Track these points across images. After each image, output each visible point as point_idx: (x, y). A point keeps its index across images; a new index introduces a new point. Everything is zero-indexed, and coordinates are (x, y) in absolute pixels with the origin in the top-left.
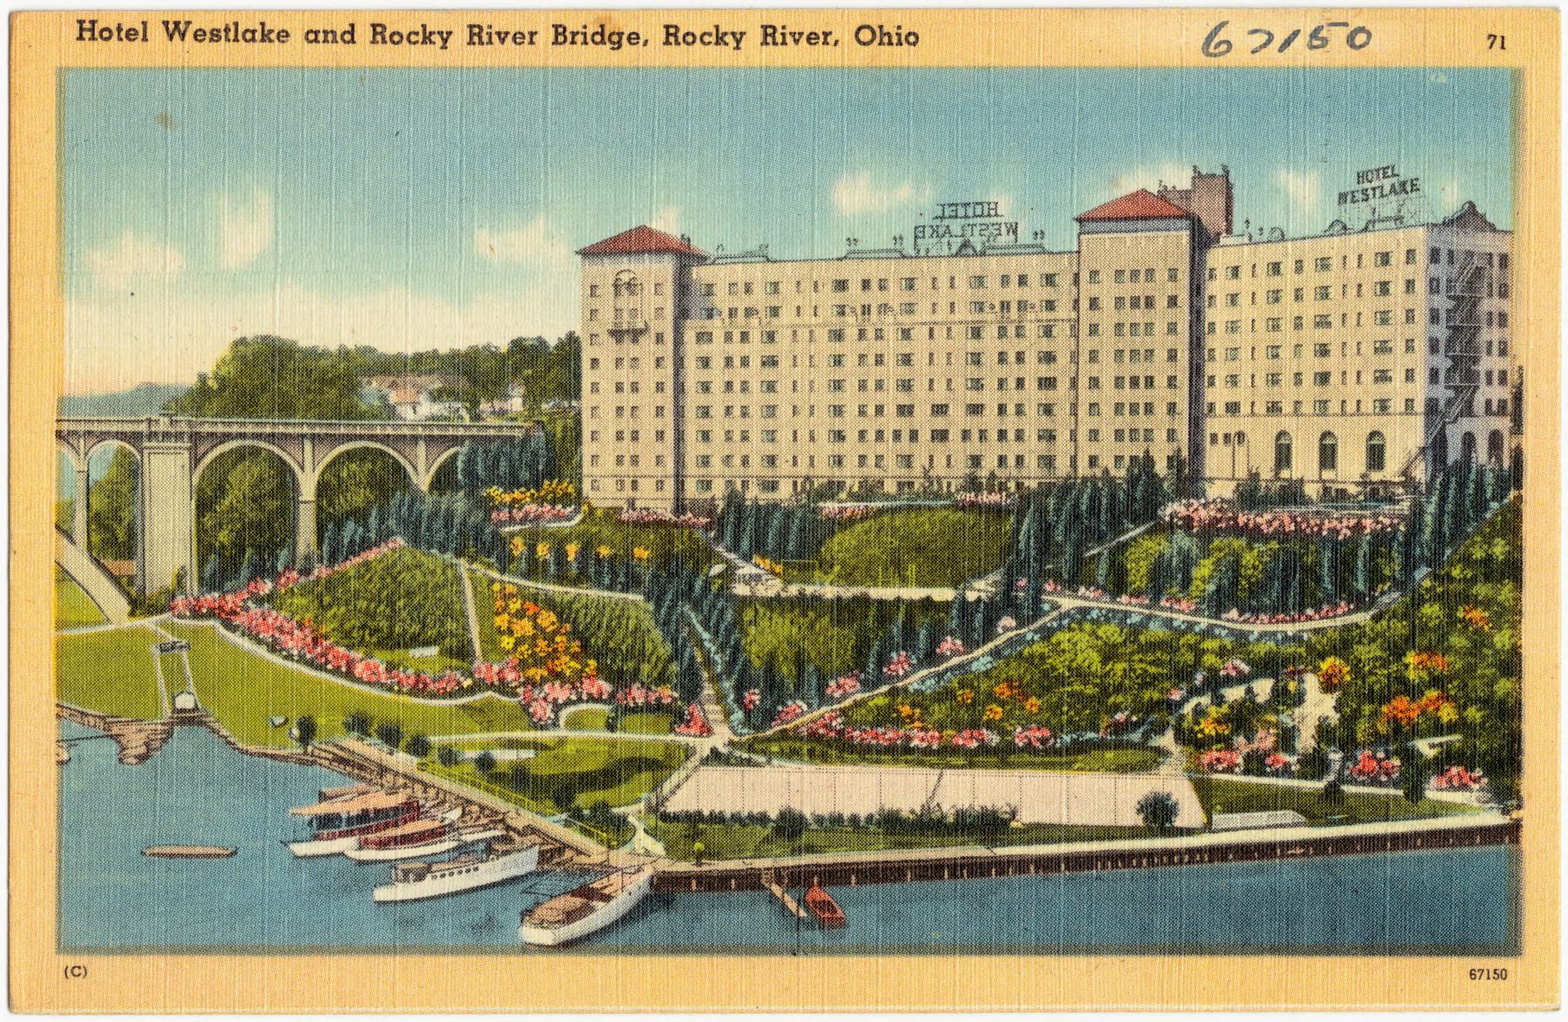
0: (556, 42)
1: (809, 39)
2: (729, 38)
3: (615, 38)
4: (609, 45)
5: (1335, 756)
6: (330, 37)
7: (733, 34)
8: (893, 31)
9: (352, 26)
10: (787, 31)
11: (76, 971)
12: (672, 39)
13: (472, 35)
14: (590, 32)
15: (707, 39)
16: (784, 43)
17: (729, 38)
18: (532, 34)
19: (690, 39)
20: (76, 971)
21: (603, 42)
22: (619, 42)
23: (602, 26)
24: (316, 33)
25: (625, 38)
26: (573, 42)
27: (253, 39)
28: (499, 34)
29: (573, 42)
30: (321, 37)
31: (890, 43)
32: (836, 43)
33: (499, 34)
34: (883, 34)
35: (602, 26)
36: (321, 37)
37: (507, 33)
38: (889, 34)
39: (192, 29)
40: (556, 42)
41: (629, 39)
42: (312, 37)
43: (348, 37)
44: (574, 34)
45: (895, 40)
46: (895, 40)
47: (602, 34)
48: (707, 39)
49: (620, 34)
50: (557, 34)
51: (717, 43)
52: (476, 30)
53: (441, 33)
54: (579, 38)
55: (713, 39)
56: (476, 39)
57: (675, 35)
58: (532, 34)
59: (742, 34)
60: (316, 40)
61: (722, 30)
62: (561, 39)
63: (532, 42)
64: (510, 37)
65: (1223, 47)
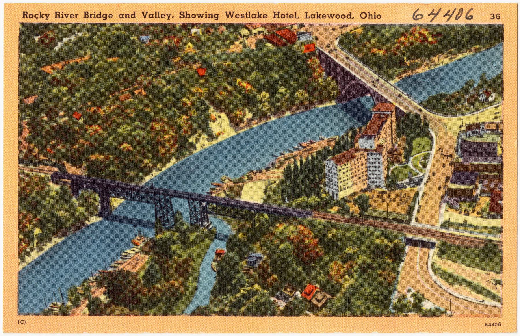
0: (85, 17)
1: (71, 16)
2: (44, 16)
3: (105, 16)
4: (102, 18)
5: (29, 250)
6: (127, 16)
7: (46, 15)
8: (373, 14)
9: (135, 12)
10: (63, 14)
11: (22, 322)
12: (25, 16)
13: (24, 15)
14: (96, 14)
15: (37, 16)
16: (62, 18)
17: (44, 16)
18: (77, 15)
19: (31, 16)
20: (22, 322)
21: (100, 17)
22: (106, 17)
23: (100, 12)
24: (123, 15)
25: (108, 16)
26: (91, 18)
27: (153, 17)
28: (65, 15)
29: (91, 18)
30: (124, 16)
31: (372, 18)
32: (173, 18)
33: (65, 15)
34: (369, 15)
35: (100, 12)
36: (124, 16)
37: (68, 15)
38: (189, 15)
39: (148, 14)
40: (85, 17)
41: (109, 16)
42: (121, 16)
43: (133, 16)
44: (91, 15)
45: (373, 17)
46: (373, 17)
47: (100, 15)
48: (37, 16)
49: (106, 15)
50: (85, 15)
51: (40, 18)
52: (58, 13)
53: (46, 15)
54: (93, 16)
55: (39, 16)
56: (58, 16)
57: (26, 15)
58: (77, 15)
59: (49, 15)
60: (123, 17)
61: (42, 13)
62: (87, 16)
63: (76, 18)
64: (69, 16)
65: (419, 17)
